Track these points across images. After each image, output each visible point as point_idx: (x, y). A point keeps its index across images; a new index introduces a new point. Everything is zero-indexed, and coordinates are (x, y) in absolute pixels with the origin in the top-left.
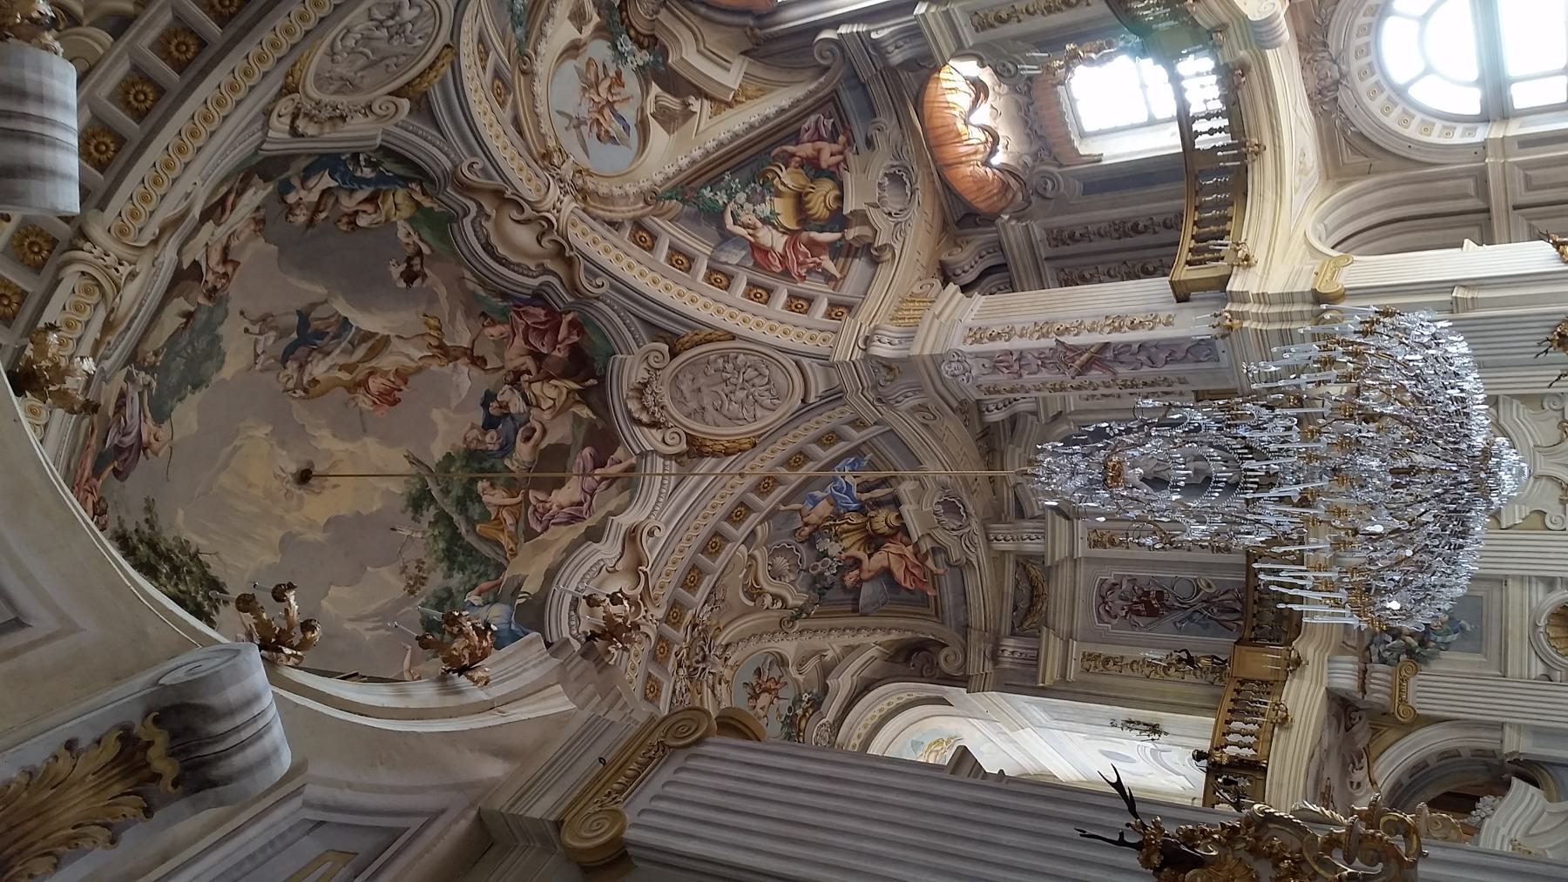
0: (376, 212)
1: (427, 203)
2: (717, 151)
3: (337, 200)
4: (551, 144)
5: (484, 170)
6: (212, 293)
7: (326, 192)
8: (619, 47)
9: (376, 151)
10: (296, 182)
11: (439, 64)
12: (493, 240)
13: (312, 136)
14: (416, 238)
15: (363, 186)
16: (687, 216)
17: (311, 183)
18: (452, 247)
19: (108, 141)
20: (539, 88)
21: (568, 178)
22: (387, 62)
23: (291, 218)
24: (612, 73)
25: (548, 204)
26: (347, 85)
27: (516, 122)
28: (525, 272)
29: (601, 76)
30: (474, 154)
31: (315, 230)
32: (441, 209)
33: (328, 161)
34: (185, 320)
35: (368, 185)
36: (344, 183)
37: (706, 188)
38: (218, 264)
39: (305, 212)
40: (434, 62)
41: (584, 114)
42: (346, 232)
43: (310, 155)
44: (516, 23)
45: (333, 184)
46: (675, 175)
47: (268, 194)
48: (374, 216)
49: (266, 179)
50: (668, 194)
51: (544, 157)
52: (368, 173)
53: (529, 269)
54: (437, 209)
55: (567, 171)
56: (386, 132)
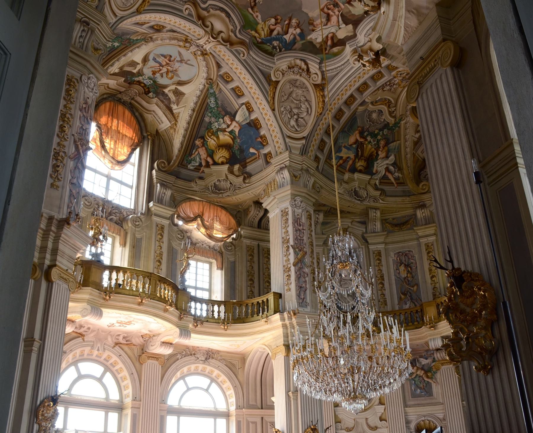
0: (269, 25)
1: (253, 33)
2: (114, 62)
3: (282, 29)
4: (201, 58)
5: (240, 54)
6: (336, 5)
7: (287, 33)
8: (152, 81)
9: (275, 54)
10: (298, 37)
11: (272, 101)
12: (227, 20)
13: (297, 59)
14: (254, 15)
15: (275, 37)
16: (128, 34)
17: (292, 37)
18: (241, 14)
19: (375, 78)
20: (205, 75)
21: (194, 47)
22: (286, 97)
23: (298, 22)
24: (158, 75)
25: (212, 44)
26: (293, 83)
27: (219, 66)
28: (213, 6)
29: (165, 75)
30: (245, 60)
31: (289, 16)
32: (248, 31)
33: (289, 47)
34: (351, 2)
35: (274, 37)
36: (281, 37)
37: (117, 46)
38: (332, 16)
39: (293, 24)
40: (274, 101)
41: (177, 65)
42: (278, 15)
43: (295, 50)
44: (214, 94)
45: (285, 37)
46: (135, 49)
47: (309, 34)
48: (270, 24)
49: (311, 43)
50: (138, 41)
51: (206, 54)
52: (275, 43)
53: (212, 8)
54: (249, 30)
55: (194, 48)
56: (274, 63)
